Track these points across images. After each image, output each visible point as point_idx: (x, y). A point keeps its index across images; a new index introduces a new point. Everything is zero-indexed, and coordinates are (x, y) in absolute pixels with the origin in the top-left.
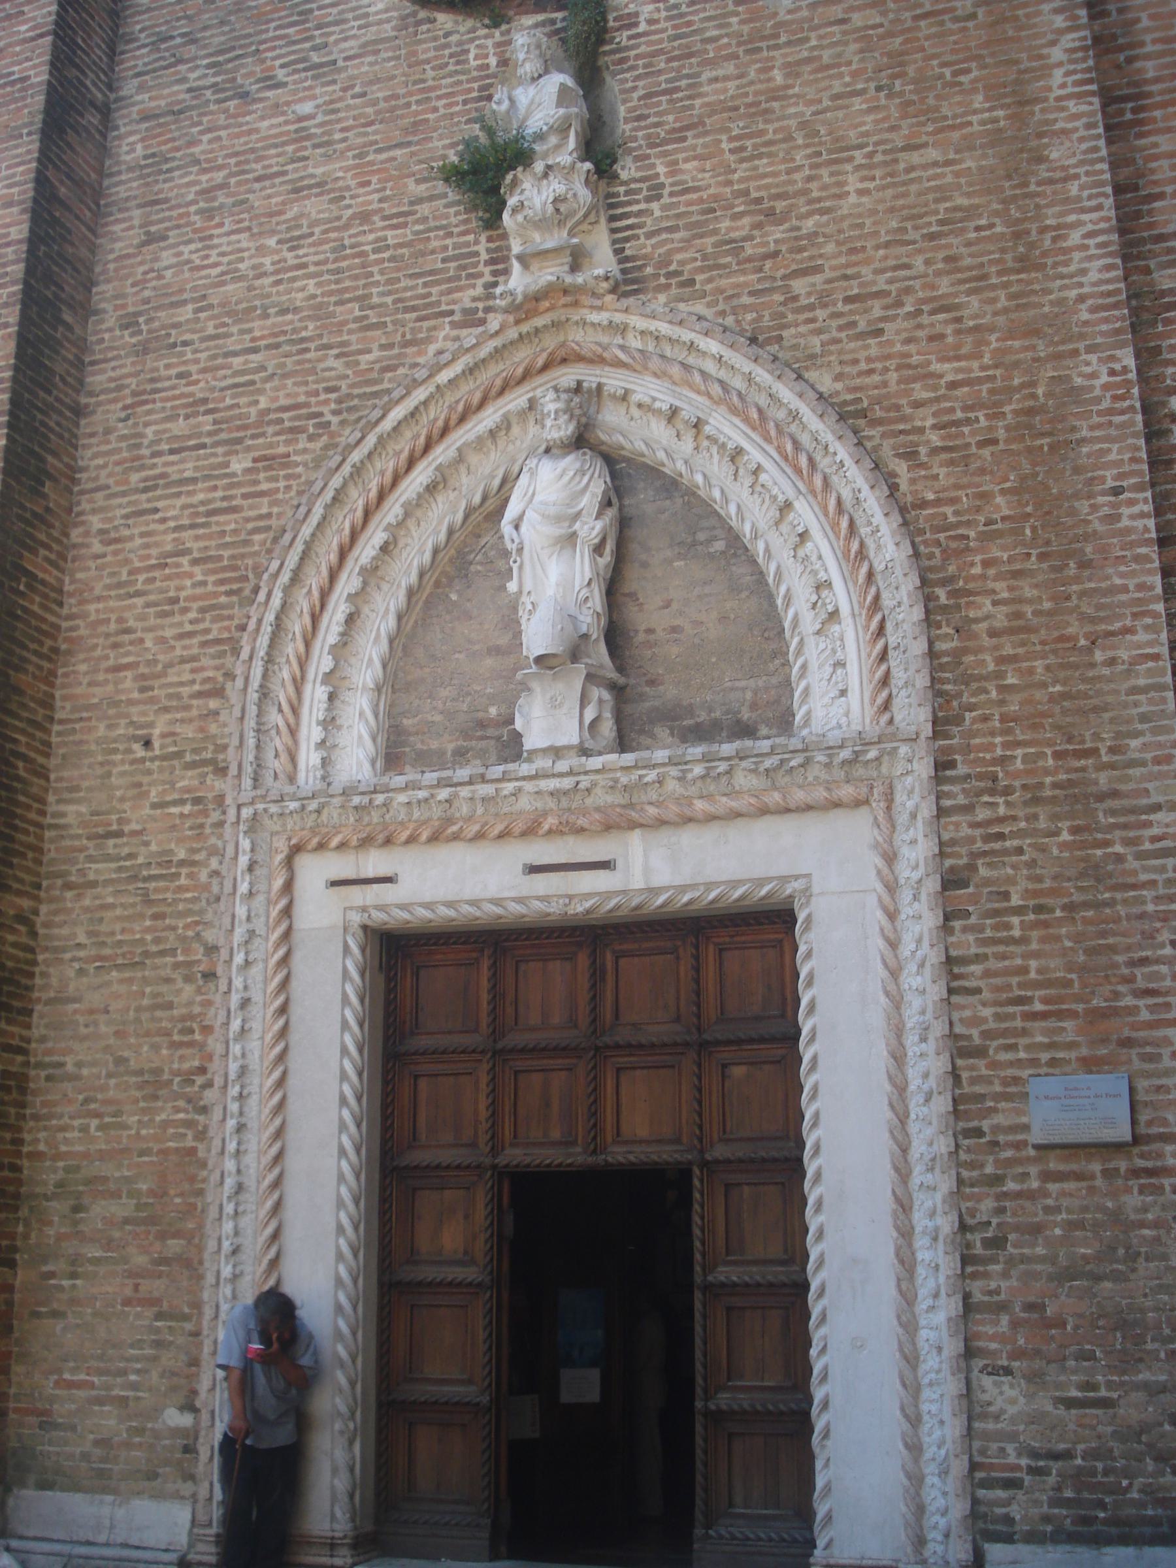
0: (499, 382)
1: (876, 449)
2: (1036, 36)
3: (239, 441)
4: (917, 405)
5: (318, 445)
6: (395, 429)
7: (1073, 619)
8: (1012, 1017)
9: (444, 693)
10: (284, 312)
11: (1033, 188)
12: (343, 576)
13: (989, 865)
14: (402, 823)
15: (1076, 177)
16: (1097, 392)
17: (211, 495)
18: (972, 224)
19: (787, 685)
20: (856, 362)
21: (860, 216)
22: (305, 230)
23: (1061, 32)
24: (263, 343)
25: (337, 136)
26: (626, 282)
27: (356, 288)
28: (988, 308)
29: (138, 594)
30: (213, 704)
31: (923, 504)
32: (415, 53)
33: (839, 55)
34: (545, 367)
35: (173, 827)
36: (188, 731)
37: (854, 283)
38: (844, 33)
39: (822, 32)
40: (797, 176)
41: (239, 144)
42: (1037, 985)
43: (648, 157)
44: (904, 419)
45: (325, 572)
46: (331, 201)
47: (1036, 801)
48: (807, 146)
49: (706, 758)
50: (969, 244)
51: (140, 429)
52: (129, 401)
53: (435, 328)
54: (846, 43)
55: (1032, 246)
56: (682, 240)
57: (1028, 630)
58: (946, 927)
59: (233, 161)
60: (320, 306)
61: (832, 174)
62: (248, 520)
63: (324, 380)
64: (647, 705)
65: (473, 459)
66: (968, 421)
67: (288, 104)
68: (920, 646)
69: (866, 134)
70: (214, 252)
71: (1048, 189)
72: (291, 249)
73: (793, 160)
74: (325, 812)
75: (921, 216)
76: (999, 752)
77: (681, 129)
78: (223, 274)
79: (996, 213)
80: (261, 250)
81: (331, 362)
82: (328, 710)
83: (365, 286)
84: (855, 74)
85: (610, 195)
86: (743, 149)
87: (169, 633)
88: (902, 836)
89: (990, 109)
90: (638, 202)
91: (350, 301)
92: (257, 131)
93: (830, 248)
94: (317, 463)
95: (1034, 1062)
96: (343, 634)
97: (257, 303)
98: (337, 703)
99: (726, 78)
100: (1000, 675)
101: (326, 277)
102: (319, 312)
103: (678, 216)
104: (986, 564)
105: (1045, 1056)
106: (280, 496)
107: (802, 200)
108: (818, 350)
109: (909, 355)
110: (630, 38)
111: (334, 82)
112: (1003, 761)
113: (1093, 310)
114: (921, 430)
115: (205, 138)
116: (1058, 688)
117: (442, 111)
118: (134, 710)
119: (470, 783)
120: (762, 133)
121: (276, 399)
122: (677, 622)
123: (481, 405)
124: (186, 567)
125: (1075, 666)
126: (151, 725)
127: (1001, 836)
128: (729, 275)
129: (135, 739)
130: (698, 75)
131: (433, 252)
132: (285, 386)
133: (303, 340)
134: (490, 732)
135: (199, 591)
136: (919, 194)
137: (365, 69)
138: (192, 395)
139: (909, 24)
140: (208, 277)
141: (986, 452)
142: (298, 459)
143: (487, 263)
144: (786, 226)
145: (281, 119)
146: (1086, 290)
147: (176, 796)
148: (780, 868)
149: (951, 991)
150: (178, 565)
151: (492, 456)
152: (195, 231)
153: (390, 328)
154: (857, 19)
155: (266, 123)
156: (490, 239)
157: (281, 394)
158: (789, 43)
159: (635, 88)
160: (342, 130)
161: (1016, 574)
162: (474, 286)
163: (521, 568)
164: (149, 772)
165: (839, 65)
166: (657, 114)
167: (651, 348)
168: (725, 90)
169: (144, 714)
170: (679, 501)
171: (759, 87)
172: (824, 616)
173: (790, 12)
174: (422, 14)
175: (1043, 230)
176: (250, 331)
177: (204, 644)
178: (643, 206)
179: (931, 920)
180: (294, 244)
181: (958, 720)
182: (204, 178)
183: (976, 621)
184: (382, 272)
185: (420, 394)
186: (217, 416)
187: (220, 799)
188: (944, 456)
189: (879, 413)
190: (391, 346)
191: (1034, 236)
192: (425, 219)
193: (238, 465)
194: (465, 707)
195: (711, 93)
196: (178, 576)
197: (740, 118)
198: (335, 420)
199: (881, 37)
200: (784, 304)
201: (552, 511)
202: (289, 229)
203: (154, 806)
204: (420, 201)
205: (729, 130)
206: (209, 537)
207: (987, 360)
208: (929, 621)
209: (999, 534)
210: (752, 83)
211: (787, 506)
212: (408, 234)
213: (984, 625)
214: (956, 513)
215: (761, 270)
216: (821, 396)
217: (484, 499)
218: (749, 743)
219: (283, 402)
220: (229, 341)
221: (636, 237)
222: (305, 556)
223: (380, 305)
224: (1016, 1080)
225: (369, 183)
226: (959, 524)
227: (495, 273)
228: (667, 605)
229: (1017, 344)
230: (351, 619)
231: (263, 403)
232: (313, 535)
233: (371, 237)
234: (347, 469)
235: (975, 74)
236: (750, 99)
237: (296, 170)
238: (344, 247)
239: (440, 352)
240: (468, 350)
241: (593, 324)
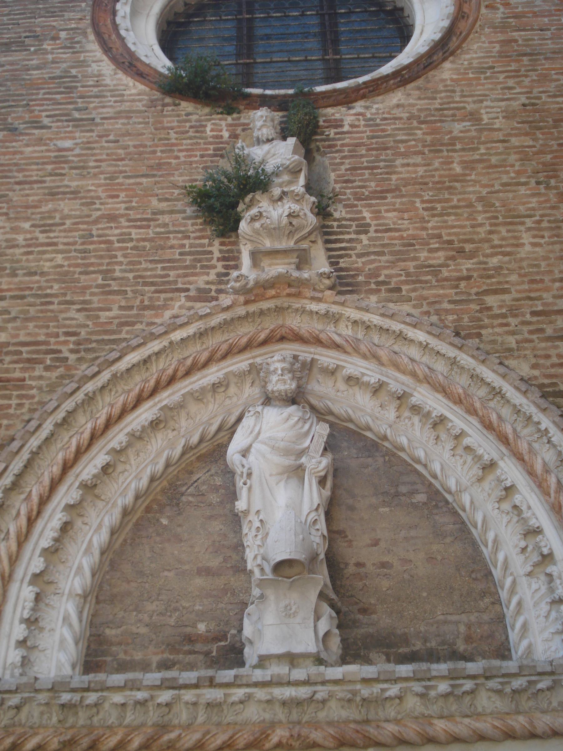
0: (225, 347)
5: (54, 374)
6: (128, 370)
9: (151, 607)
12: (62, 489)
14: (110, 727)
19: (501, 619)
20: (548, 357)
21: (536, 259)
22: (57, 220)
24: (8, 294)
25: (92, 164)
26: (341, 285)
27: (102, 264)
32: (161, 122)
33: (505, 160)
34: (264, 343)
37: (539, 303)
38: (506, 148)
39: (489, 145)
43: (356, 206)
45: (46, 481)
46: (82, 204)
48: (486, 212)
49: (452, 676)
53: (172, 299)
54: (509, 154)
56: (387, 262)
60: (67, 273)
61: (508, 231)
63: (64, 326)
64: (362, 631)
65: (193, 407)
67: (51, 139)
69: (533, 209)
72: (42, 232)
73: (475, 219)
74: (25, 710)
77: (382, 192)
80: (15, 230)
82: (34, 609)
83: (108, 264)
84: (518, 173)
85: (324, 226)
86: (433, 209)
90: (349, 233)
92: (21, 153)
93: (514, 278)
94: (52, 388)
96: (56, 540)
97: (8, 265)
98: (42, 605)
99: (415, 165)
101: (73, 254)
103: (383, 246)
106: (12, 411)
107: (486, 245)
108: (514, 345)
110: (336, 134)
111: (92, 131)
117: (183, 159)
119: (196, 686)
120: (447, 201)
121: (17, 336)
122: (386, 559)
123: (206, 365)
128: (430, 288)
130: (394, 161)
131: (172, 247)
132: (26, 328)
133: (47, 296)
134: (198, 647)
137: (119, 126)
142: (33, 383)
143: (219, 260)
144: (475, 260)
145: (44, 148)
151: (211, 406)
153: (130, 295)
154: (515, 141)
155: (30, 149)
156: (222, 244)
157: (22, 332)
159: (342, 163)
160: (96, 161)
162: (208, 274)
163: (250, 489)
166: (360, 181)
167: (360, 336)
170: (381, 460)
171: (442, 172)
172: (536, 558)
173: (461, 132)
174: (168, 100)
178: (353, 236)
180: (46, 229)
184: (125, 256)
185: (155, 346)
190: (131, 308)
192: (165, 225)
194: (172, 622)
195: (405, 173)
197: (430, 189)
198: (72, 357)
199: (535, 153)
200: (480, 311)
201: (282, 444)
202: (43, 218)
204: (162, 213)
205: (420, 196)
210: (436, 170)
211: (491, 466)
215: (457, 287)
217: (201, 441)
218: (496, 663)
222: (28, 465)
223: (122, 279)
225: (118, 196)
227: (226, 267)
228: (376, 543)
230: (66, 527)
232: (40, 447)
233: (117, 231)
234: (80, 396)
236: (437, 179)
237: (54, 181)
238: (92, 236)
239: (175, 317)
240: (201, 317)
241: (311, 312)
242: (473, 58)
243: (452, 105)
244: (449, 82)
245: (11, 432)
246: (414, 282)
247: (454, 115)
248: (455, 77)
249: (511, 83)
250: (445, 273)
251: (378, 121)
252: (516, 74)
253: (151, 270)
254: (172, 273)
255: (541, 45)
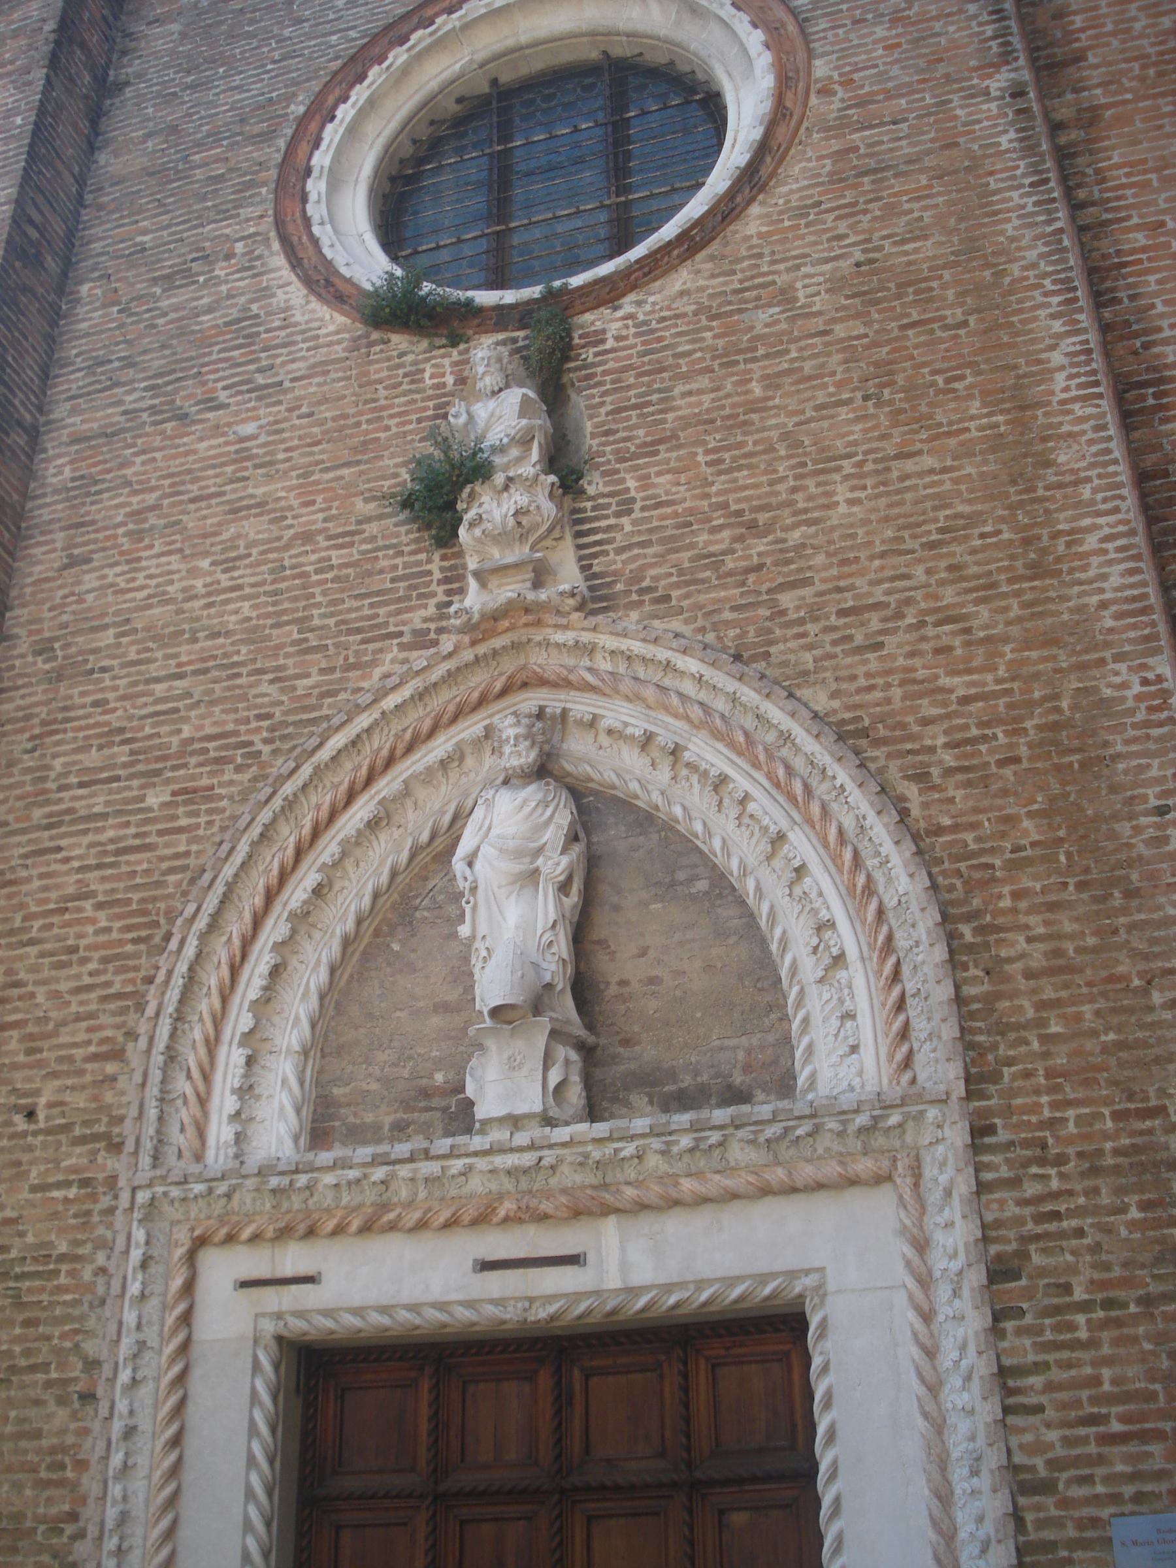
0: (451, 708)
1: (881, 771)
2: (1033, 341)
3: (157, 773)
4: (926, 722)
5: (246, 776)
6: (333, 759)
7: (1122, 956)
9: (382, 1057)
10: (215, 635)
11: (1040, 492)
12: (270, 922)
13: (1044, 1251)
14: (328, 1210)
15: (1088, 480)
16: (1130, 703)
17: (122, 832)
18: (976, 531)
19: (786, 1041)
20: (853, 678)
21: (852, 526)
22: (242, 551)
23: (1059, 336)
24: (189, 668)
25: (281, 456)
26: (595, 599)
27: (296, 610)
28: (1000, 618)
29: (32, 942)
30: (110, 1068)
31: (939, 830)
32: (367, 374)
33: (823, 366)
34: (504, 693)
35: (55, 1215)
36: (79, 1100)
37: (849, 595)
38: (827, 344)
39: (802, 343)
40: (780, 487)
41: (175, 466)
42: (1111, 1399)
43: (617, 471)
44: (911, 737)
45: (248, 917)
46: (271, 522)
47: (1095, 1171)
48: (790, 457)
49: (695, 1127)
50: (974, 552)
51: (48, 761)
52: (37, 731)
53: (381, 650)
54: (829, 355)
55: (1043, 552)
56: (655, 556)
57: (1070, 969)
58: (996, 1331)
59: (167, 482)
61: (818, 485)
62: (162, 859)
63: (256, 707)
64: (622, 1068)
65: (421, 793)
66: (985, 738)
67: (229, 425)
68: (945, 991)
69: (855, 443)
70: (141, 575)
71: (1058, 494)
72: (225, 571)
73: (775, 471)
74: (236, 1197)
75: (919, 525)
76: (1047, 1113)
77: (653, 443)
78: (150, 597)
79: (1002, 519)
80: (193, 573)
81: (264, 688)
82: (246, 1076)
83: (305, 608)
84: (839, 385)
85: (575, 511)
86: (720, 461)
87: (64, 987)
88: (934, 1219)
89: (988, 415)
90: (607, 517)
91: (288, 623)
92: (195, 452)
93: (820, 560)
94: (244, 797)
95: (1116, 1499)
96: (266, 989)
97: (186, 626)
98: (256, 1069)
99: (700, 392)
100: (1041, 1023)
101: (263, 599)
102: (254, 636)
103: (651, 531)
104: (1017, 895)
105: (1128, 1490)
106: (201, 832)
107: (787, 511)
108: (811, 666)
109: (913, 670)
110: (596, 355)
111: (280, 403)
112: (1052, 1124)
113: (1118, 616)
114: (932, 750)
115: (138, 460)
116: (1112, 1036)
117: (394, 430)
118: (18, 1075)
119: (411, 1159)
121: (202, 727)
122: (654, 973)
123: (432, 733)
124: (89, 912)
125: (1131, 1011)
126: (37, 1093)
127: (1056, 1216)
128: (708, 590)
129: (17, 1109)
131: (381, 572)
132: (211, 714)
134: (436, 1102)
135: (102, 938)
136: (916, 502)
137: (312, 390)
138: (108, 723)
139: (896, 333)
140: (134, 600)
141: (1008, 772)
142: (223, 791)
143: (440, 582)
144: (770, 538)
145: (222, 440)
146: (1108, 596)
147: (61, 1177)
148: (787, 1261)
149: (1006, 1410)
150: (80, 910)
151: (443, 788)
152: (122, 553)
153: (332, 649)
154: (840, 330)
155: (204, 444)
156: (444, 558)
157: (207, 722)
158: (767, 356)
159: (603, 404)
160: (286, 450)
161: (1052, 907)
162: (425, 607)
163: (474, 909)
164: (30, 1149)
165: (821, 376)
166: (625, 429)
167: (622, 670)
168: (700, 404)
169: (28, 1080)
170: (655, 837)
171: (736, 399)
172: (827, 961)
173: (767, 325)
174: (375, 336)
175: (1055, 536)
176: (175, 656)
177: (104, 999)
178: (612, 521)
179: (976, 1321)
180: (229, 565)
181: (996, 1077)
182: (135, 500)
183: (1010, 960)
184: (324, 593)
185: (363, 721)
186: (135, 746)
187: (112, 1180)
188: (960, 777)
189: (882, 732)
190: (332, 670)
191: (1045, 541)
192: (373, 538)
193: (154, 799)
194: (406, 1073)
195: (684, 407)
196: (79, 922)
197: (717, 430)
198: (266, 749)
199: (867, 347)
200: (771, 618)
201: (511, 844)
202: (224, 551)
203: (34, 1189)
204: (368, 519)
205: (704, 443)
206: (118, 878)
207: (1001, 672)
208: (954, 962)
209: (1029, 861)
210: (728, 396)
211: (780, 839)
212: (354, 553)
213: (1019, 965)
214: (978, 839)
215: (743, 584)
216: (816, 716)
217: (433, 836)
218: (745, 1108)
219: (209, 730)
220: (152, 666)
221: (605, 553)
222: (225, 900)
223: (321, 628)
224: (1095, 1522)
225: (313, 502)
226: (982, 852)
227: (449, 593)
228: (643, 953)
229: (1034, 654)
230: (276, 972)
231: (187, 731)
232: (236, 875)
233: (314, 557)
234: (277, 802)
235: (970, 380)
236: (727, 412)
237: (235, 491)
238: (284, 568)
239: (386, 676)
240: (418, 673)
241: (557, 645)
242: (792, 192)
243: (757, 281)
244: (755, 241)
245: (201, 861)
246: (687, 583)
247: (758, 298)
248: (764, 229)
249: (842, 227)
250: (730, 564)
251: (654, 325)
252: (851, 211)
253: (357, 609)
254: (382, 611)
255: (891, 150)
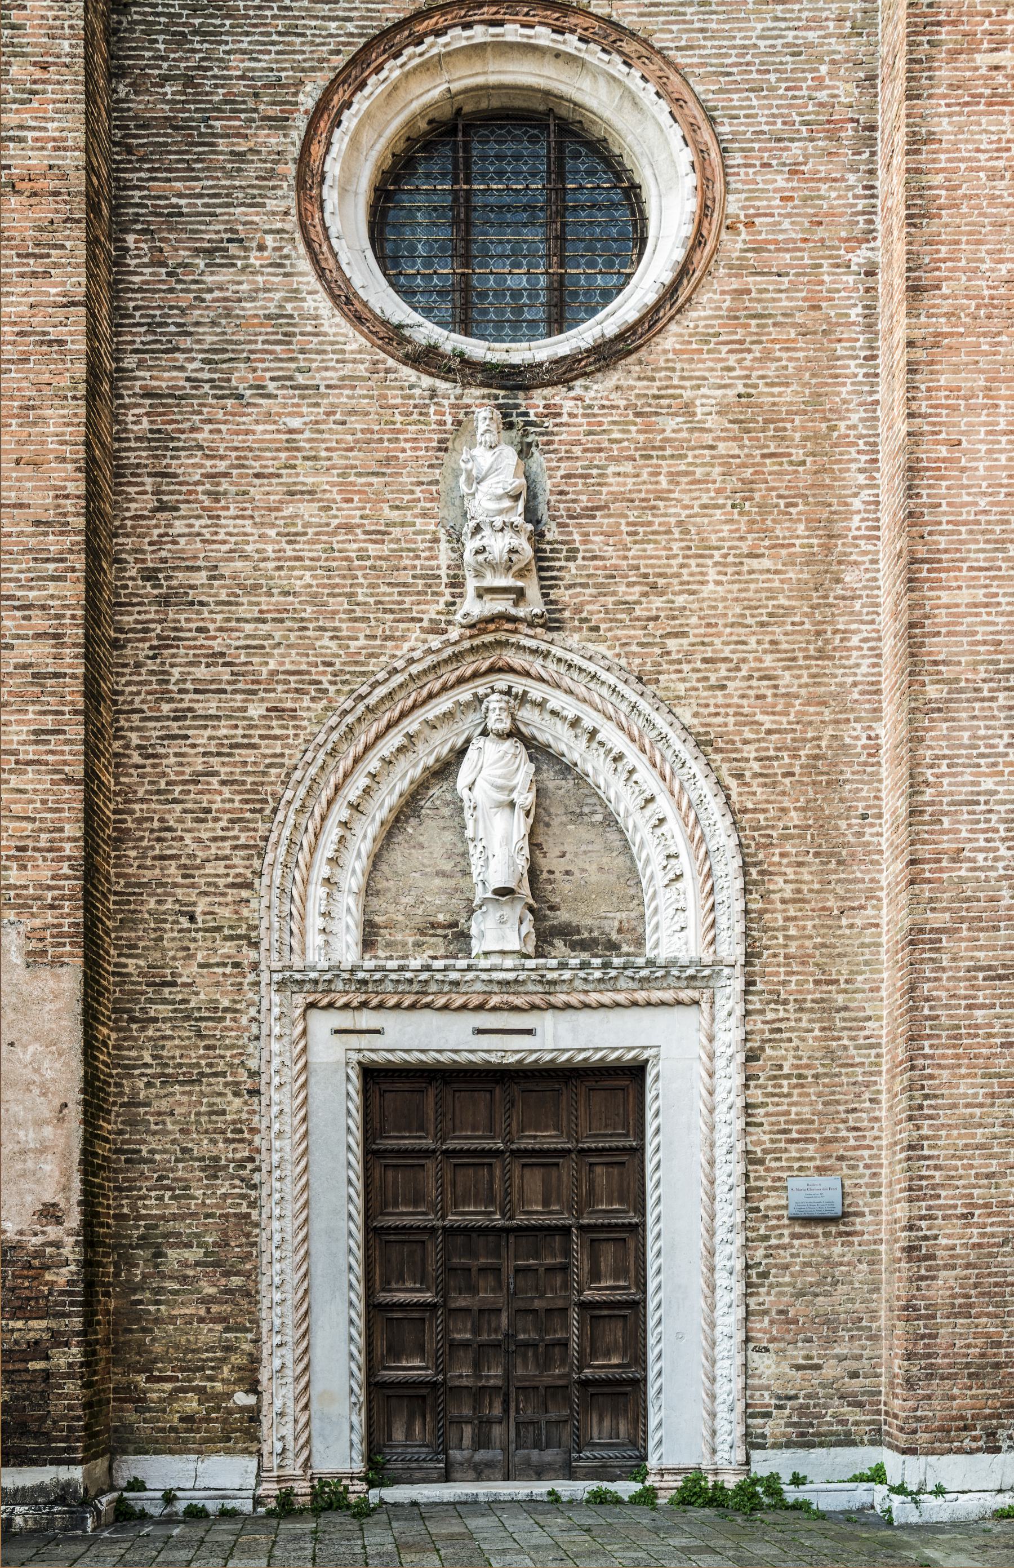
1: (718, 769)
2: (844, 487)
3: (254, 692)
4: (746, 742)
8: (779, 1141)
10: (287, 594)
11: (831, 600)
15: (860, 597)
16: (859, 750)
17: (233, 732)
18: (789, 620)
20: (707, 706)
22: (299, 529)
23: (861, 487)
24: (269, 616)
25: (324, 454)
27: (344, 586)
28: (796, 682)
29: (175, 801)
30: (245, 894)
31: (745, 811)
38: (713, 457)
39: (697, 452)
40: (673, 562)
41: (237, 441)
42: (796, 1122)
43: (567, 525)
44: (736, 750)
46: (320, 509)
50: (786, 634)
51: (167, 668)
52: (155, 643)
55: (827, 642)
57: (804, 901)
59: (234, 454)
60: (315, 595)
62: (265, 756)
66: (777, 758)
67: (279, 414)
68: (740, 906)
70: (222, 531)
71: (842, 603)
72: (290, 542)
75: (757, 608)
76: (782, 978)
77: (592, 509)
78: (231, 551)
79: (806, 615)
81: (326, 642)
84: (718, 491)
86: (636, 533)
87: (205, 835)
88: (719, 1026)
89: (808, 537)
91: (340, 595)
92: (253, 432)
93: (694, 620)
99: (626, 475)
100: (785, 928)
103: (588, 576)
104: (782, 855)
107: (675, 581)
108: (682, 693)
109: (742, 706)
112: (784, 983)
113: (863, 693)
114: (747, 760)
115: (208, 427)
118: (179, 891)
120: (650, 524)
124: (216, 786)
126: (194, 904)
127: (779, 1030)
129: (183, 914)
130: (606, 467)
132: (289, 655)
133: (302, 620)
135: (228, 806)
136: (756, 592)
137: (344, 400)
138: (211, 647)
139: (758, 459)
140: (218, 551)
141: (787, 781)
142: (304, 714)
145: (273, 427)
146: (859, 678)
147: (218, 960)
149: (747, 1124)
150: (208, 783)
152: (203, 509)
153: (373, 623)
154: (722, 448)
155: (260, 428)
158: (672, 456)
160: (327, 449)
161: (800, 864)
164: (195, 940)
165: (707, 482)
168: (625, 484)
169: (188, 895)
175: (835, 632)
176: (258, 604)
177: (235, 848)
178: (563, 563)
181: (759, 956)
182: (209, 463)
183: (773, 892)
184: (365, 576)
186: (235, 669)
188: (761, 780)
189: (721, 745)
190: (374, 637)
191: (829, 635)
196: (209, 791)
197: (636, 508)
198: (332, 689)
200: (661, 656)
203: (201, 966)
204: (394, 525)
205: (626, 516)
206: (234, 764)
207: (792, 718)
209: (791, 837)
212: (385, 549)
213: (778, 895)
214: (766, 819)
215: (646, 628)
216: (684, 728)
219: (289, 667)
220: (241, 609)
221: (557, 586)
225: (351, 501)
226: (767, 827)
229: (812, 709)
231: (272, 665)
233: (355, 546)
235: (801, 508)
236: (643, 495)
242: (700, 318)
243: (670, 391)
244: (671, 356)
246: (611, 620)
247: (670, 406)
248: (678, 347)
249: (732, 360)
250: (638, 612)
251: (596, 411)
252: (740, 347)
253: (391, 594)
254: (407, 599)
255: (774, 300)
